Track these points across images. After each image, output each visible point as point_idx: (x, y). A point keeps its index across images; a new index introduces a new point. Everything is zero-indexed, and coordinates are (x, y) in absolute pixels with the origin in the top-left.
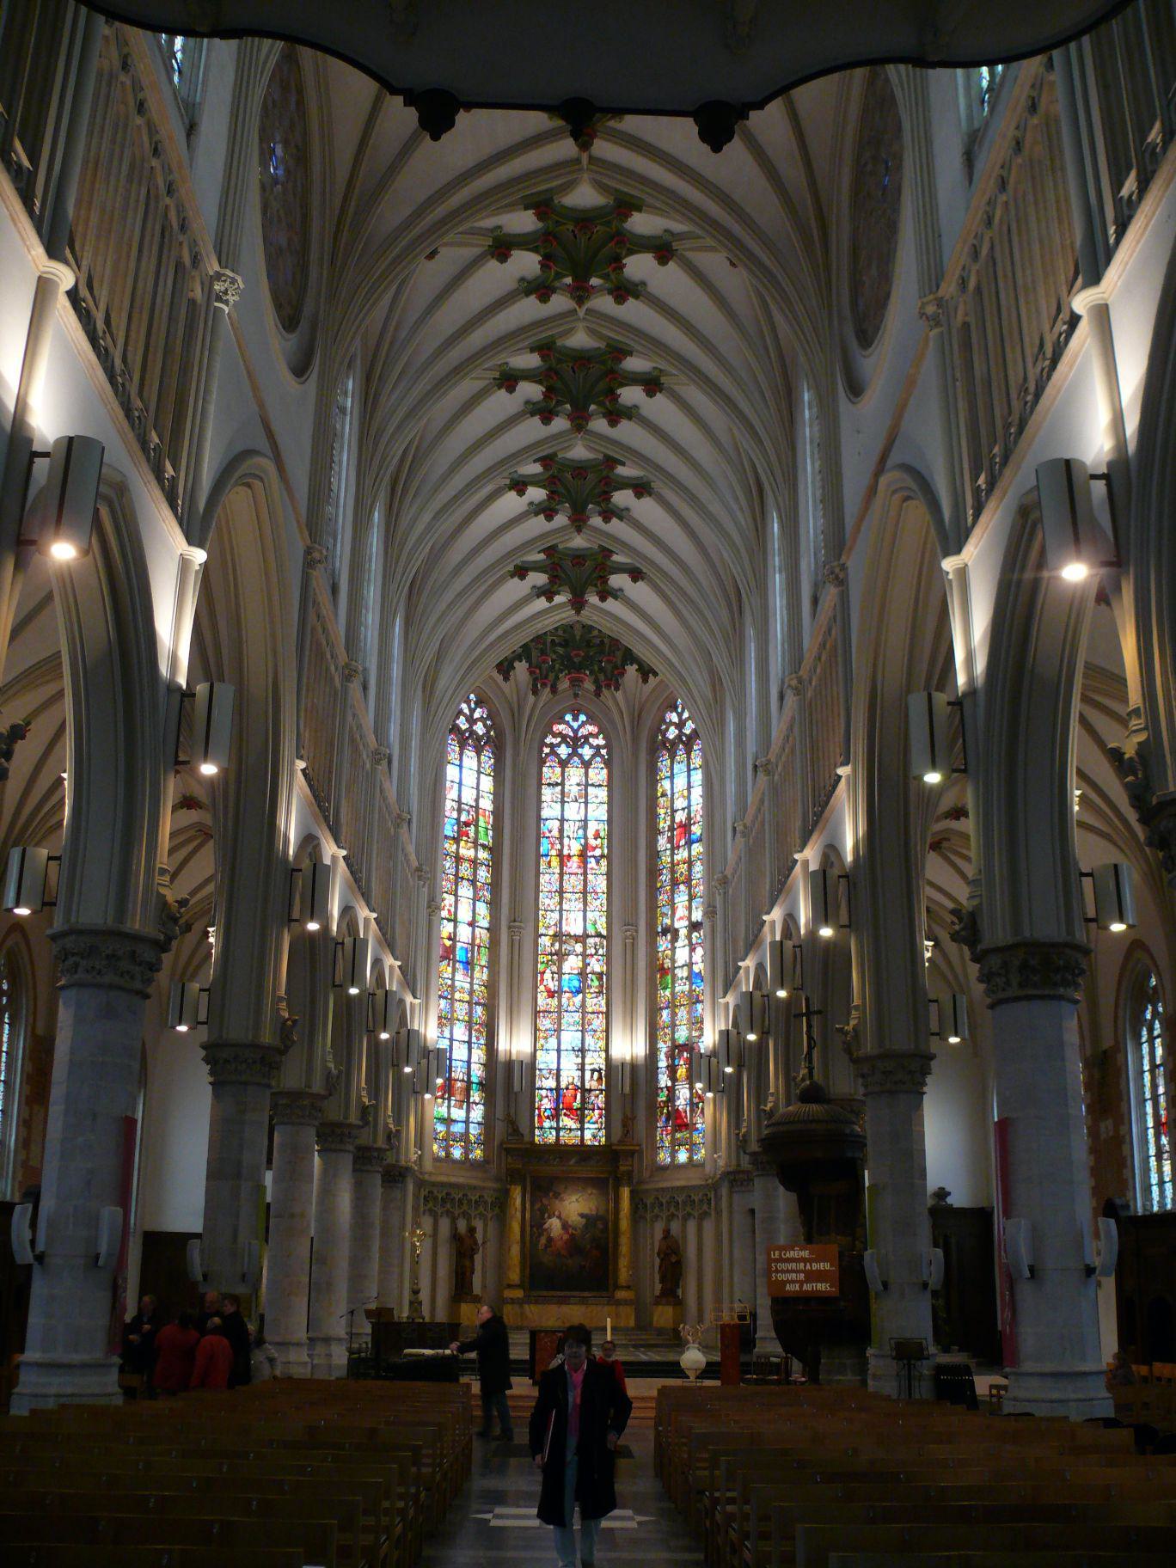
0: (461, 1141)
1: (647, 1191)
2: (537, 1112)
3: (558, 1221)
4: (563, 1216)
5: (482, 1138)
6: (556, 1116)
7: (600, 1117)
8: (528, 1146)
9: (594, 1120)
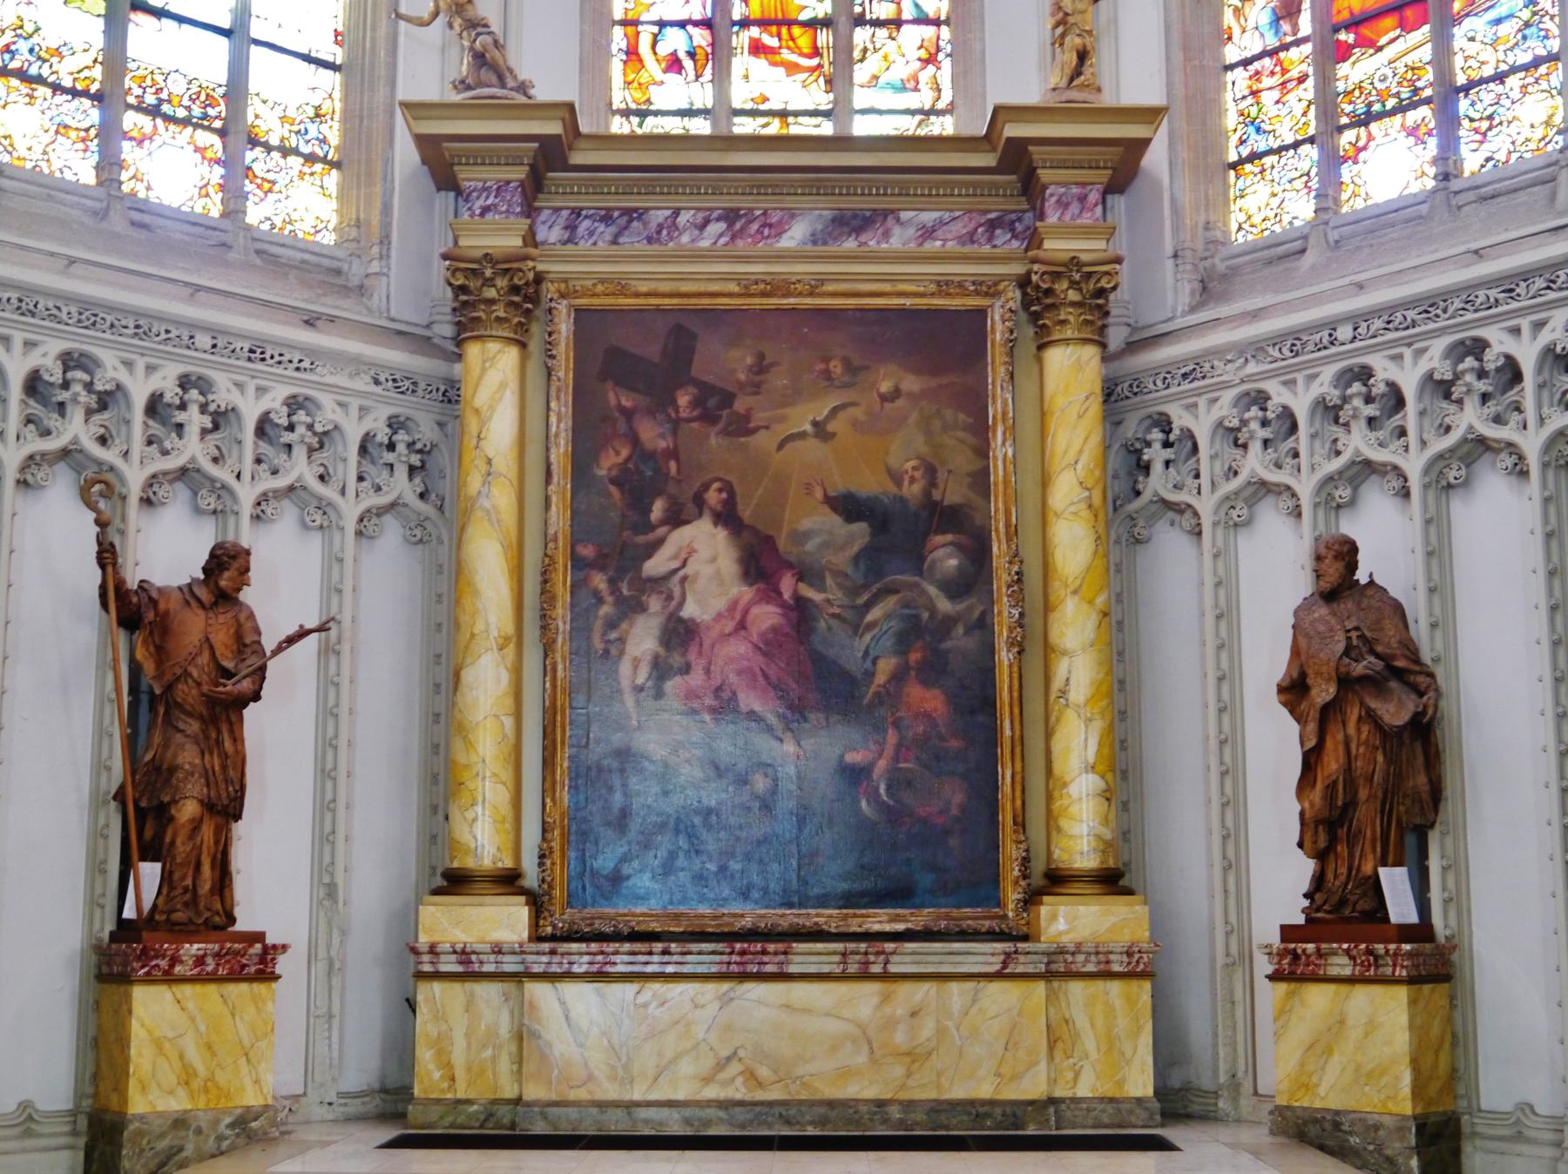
0: (202, 123)
1: (1192, 371)
2: (618, 37)
3: (721, 534)
4: (746, 512)
5: (333, 132)
6: (717, 57)
7: (931, 60)
8: (553, 128)
9: (900, 72)
